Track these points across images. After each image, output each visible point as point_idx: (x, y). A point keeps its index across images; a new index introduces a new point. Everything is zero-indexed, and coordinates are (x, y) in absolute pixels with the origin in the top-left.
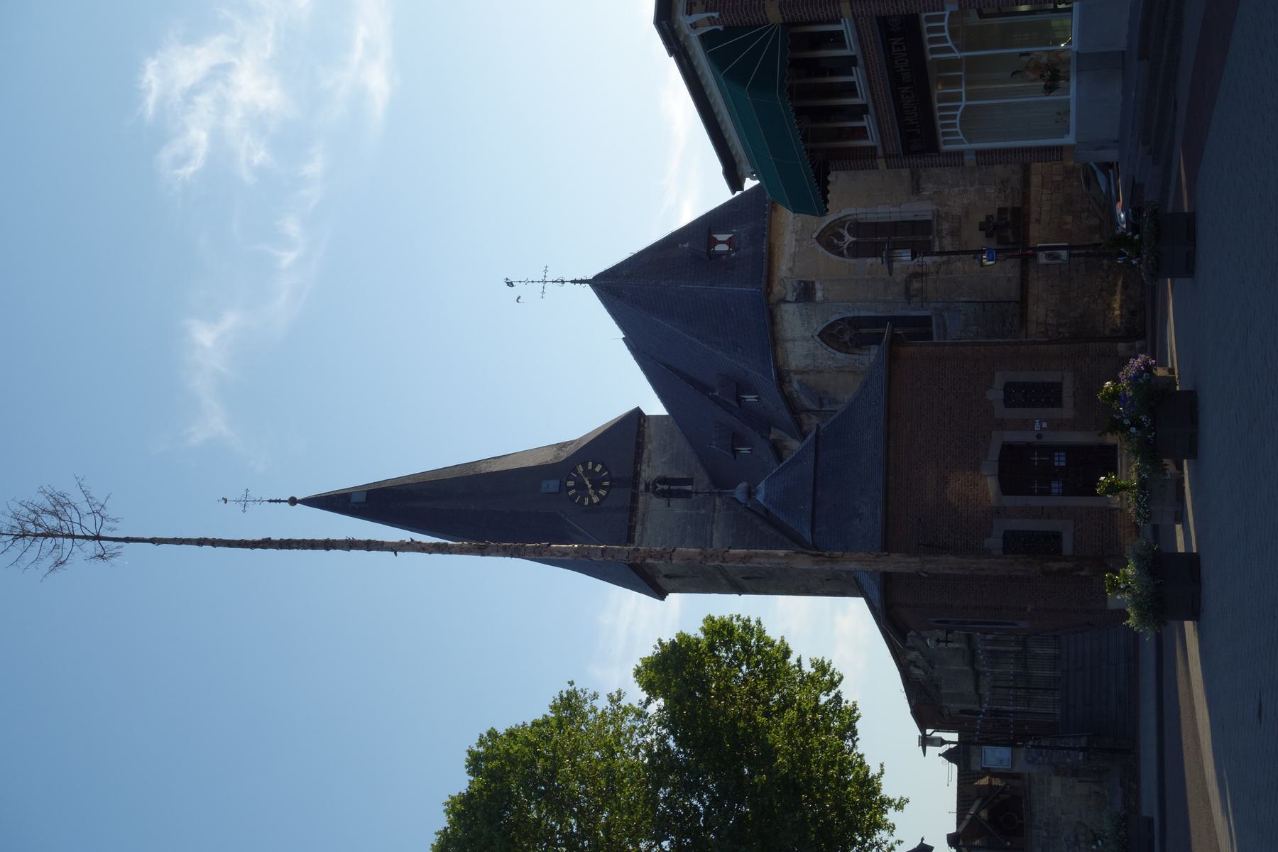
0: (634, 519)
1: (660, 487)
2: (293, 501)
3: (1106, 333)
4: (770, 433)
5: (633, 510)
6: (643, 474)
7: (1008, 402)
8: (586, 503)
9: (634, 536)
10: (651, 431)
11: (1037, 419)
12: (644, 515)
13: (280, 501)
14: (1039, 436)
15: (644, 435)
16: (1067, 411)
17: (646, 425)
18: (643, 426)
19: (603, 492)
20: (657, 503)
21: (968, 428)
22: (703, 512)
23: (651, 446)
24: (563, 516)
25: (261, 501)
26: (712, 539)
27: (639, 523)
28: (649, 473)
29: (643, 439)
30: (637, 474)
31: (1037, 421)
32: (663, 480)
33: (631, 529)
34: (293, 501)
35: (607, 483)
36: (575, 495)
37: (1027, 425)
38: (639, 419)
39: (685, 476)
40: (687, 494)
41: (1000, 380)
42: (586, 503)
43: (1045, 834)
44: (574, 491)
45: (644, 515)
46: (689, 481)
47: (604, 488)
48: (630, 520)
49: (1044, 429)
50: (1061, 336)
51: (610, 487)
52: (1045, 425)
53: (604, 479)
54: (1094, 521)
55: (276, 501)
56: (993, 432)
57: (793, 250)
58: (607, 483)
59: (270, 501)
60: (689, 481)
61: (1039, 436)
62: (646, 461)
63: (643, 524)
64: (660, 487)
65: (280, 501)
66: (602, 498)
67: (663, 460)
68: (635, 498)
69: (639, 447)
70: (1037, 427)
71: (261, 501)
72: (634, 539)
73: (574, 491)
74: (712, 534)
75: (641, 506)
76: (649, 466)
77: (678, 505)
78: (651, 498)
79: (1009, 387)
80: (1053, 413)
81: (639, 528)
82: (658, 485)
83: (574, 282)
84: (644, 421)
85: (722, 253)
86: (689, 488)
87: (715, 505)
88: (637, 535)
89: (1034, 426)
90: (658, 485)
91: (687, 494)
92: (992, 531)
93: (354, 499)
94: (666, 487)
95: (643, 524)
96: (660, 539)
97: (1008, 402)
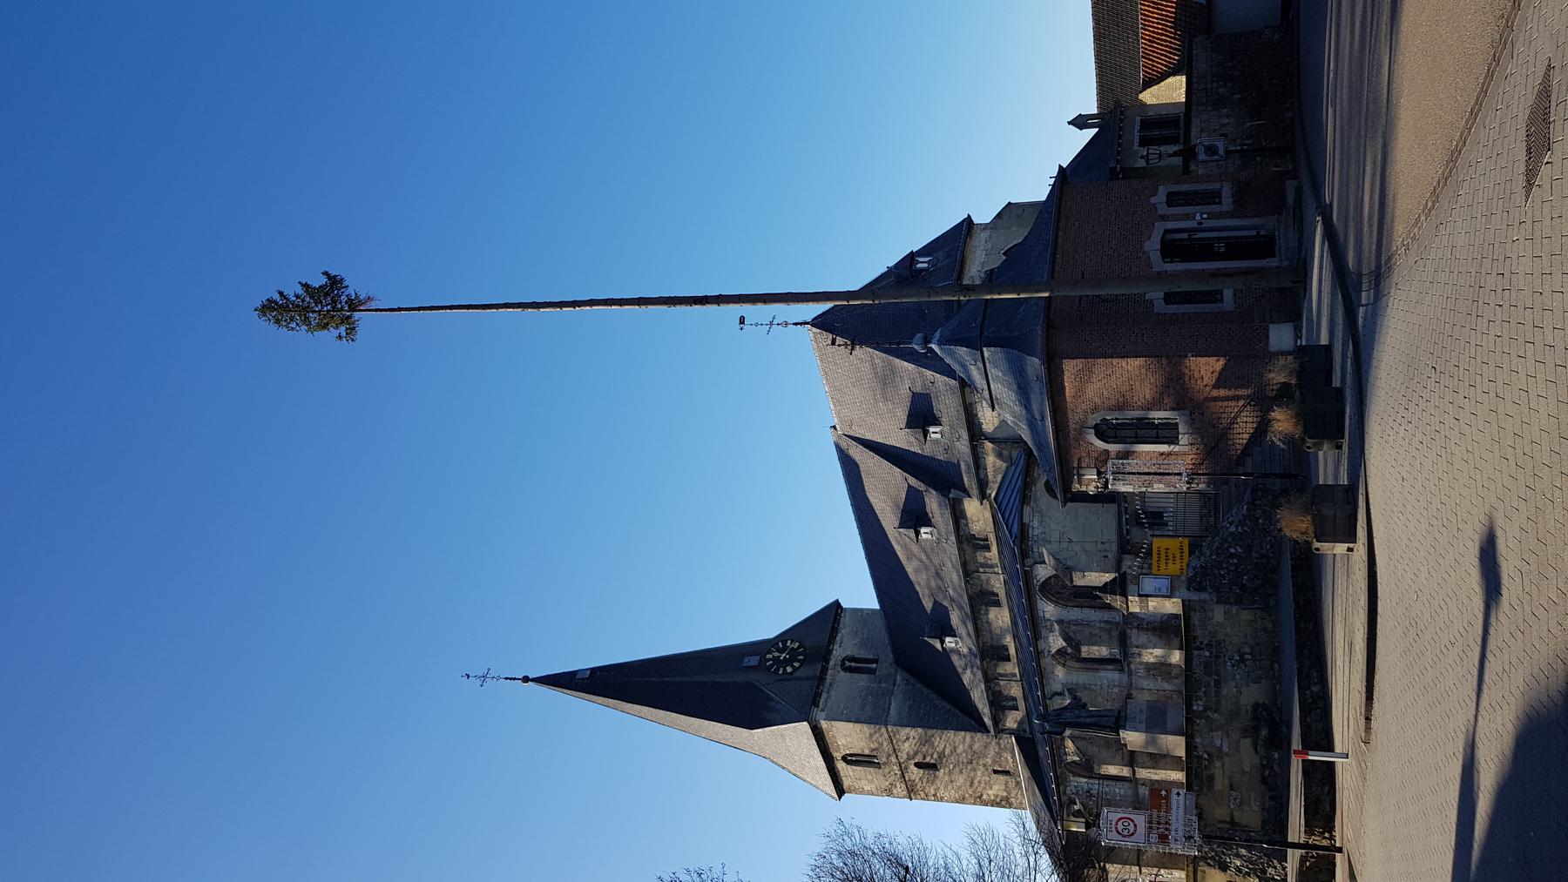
0: (821, 687)
1: (848, 664)
2: (526, 679)
4: (950, 492)
5: (821, 679)
6: (834, 652)
7: (1170, 203)
8: (781, 672)
9: (819, 701)
10: (845, 620)
12: (831, 685)
13: (515, 679)
14: (1200, 223)
15: (839, 622)
16: (1227, 204)
19: (796, 665)
23: (845, 632)
24: (757, 684)
25: (499, 678)
26: (889, 709)
27: (825, 691)
28: (838, 652)
29: (838, 625)
30: (829, 652)
33: (818, 695)
34: (526, 679)
35: (801, 657)
36: (772, 666)
37: (1188, 217)
39: (871, 657)
42: (781, 672)
43: (1208, 654)
44: (771, 662)
45: (831, 685)
46: (875, 661)
47: (799, 661)
48: (818, 687)
51: (804, 660)
55: (511, 679)
57: (982, 260)
58: (801, 657)
59: (506, 678)
63: (828, 693)
64: (848, 664)
65: (515, 679)
66: (795, 669)
67: (854, 642)
68: (824, 670)
69: (834, 631)
70: (1198, 217)
71: (499, 678)
73: (771, 662)
74: (891, 704)
77: (862, 680)
78: (838, 672)
79: (1170, 195)
80: (1214, 208)
81: (824, 695)
82: (846, 662)
83: (794, 324)
84: (841, 612)
85: (922, 270)
86: (874, 665)
87: (895, 681)
88: (822, 700)
90: (846, 662)
91: (872, 672)
93: (579, 676)
94: (853, 664)
95: (828, 693)
97: (1170, 203)
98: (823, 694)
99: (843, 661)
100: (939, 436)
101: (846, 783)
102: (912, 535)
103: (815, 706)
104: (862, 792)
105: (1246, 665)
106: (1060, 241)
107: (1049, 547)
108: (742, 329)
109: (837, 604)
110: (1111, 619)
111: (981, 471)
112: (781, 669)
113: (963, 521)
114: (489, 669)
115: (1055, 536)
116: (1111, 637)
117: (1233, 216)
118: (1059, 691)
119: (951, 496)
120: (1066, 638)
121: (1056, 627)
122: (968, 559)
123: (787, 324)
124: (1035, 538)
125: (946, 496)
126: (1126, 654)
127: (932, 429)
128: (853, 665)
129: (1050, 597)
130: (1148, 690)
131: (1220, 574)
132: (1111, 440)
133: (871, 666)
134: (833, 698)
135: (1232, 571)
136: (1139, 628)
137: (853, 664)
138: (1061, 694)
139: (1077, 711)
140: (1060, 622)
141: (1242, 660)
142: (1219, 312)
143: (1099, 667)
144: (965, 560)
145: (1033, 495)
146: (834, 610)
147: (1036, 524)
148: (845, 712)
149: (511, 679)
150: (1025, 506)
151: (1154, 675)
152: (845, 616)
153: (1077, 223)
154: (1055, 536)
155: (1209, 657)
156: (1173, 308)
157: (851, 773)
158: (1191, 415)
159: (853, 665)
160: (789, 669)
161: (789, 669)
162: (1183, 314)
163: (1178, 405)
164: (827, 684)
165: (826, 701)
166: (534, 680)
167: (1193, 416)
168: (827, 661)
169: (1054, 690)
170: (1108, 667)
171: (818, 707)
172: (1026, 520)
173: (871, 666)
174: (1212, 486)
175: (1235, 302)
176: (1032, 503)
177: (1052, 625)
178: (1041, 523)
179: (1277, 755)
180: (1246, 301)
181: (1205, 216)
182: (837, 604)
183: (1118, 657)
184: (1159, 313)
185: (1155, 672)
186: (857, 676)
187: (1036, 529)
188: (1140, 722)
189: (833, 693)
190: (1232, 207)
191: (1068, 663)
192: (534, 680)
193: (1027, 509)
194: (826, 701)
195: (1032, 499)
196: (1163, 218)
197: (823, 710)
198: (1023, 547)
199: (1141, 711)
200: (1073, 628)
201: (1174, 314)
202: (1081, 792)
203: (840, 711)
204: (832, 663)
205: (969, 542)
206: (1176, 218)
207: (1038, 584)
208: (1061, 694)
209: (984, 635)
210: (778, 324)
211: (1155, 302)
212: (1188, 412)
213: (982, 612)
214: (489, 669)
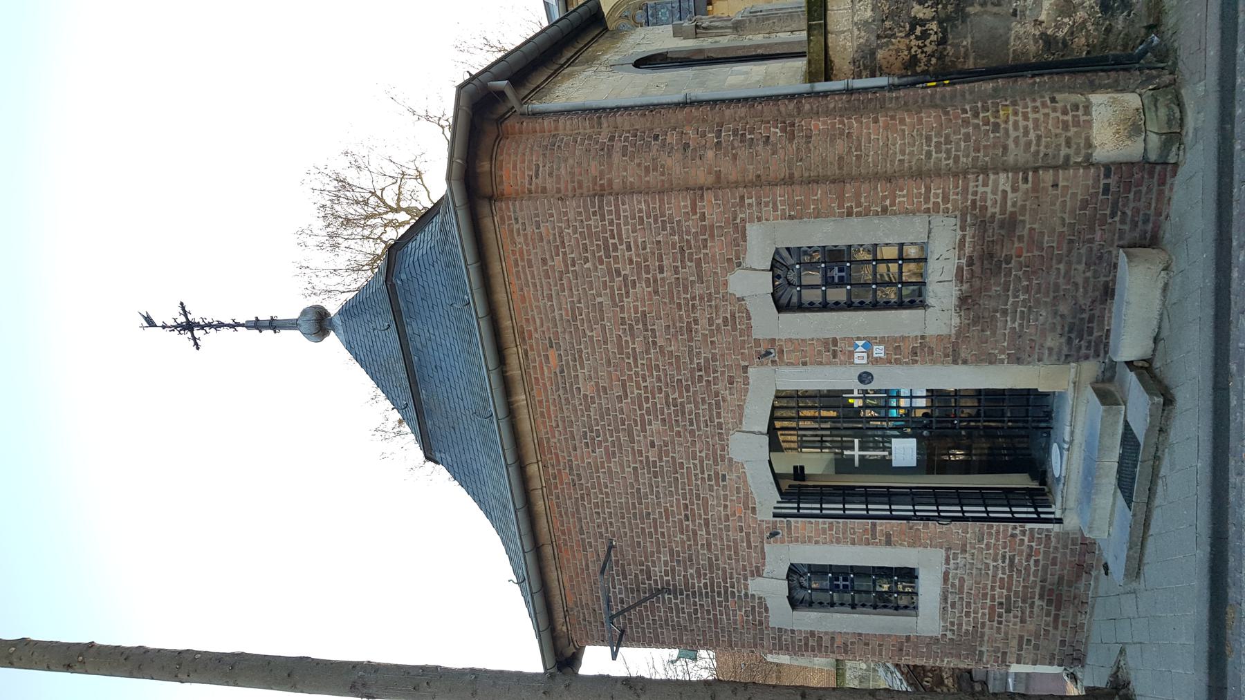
3: (1043, 17)
11: (859, 339)
14: (865, 378)
21: (691, 362)
31: (860, 343)
37: (833, 350)
41: (759, 251)
43: (864, 666)
49: (877, 361)
50: (919, 29)
52: (879, 351)
54: (991, 551)
56: (750, 370)
61: (865, 378)
70: (860, 358)
89: (852, 354)
92: (764, 565)
106: (525, 426)
117: (955, 357)
142: (908, 638)
153: (552, 353)
155: (866, 670)
156: (809, 620)
175: (944, 619)
180: (968, 614)
181: (879, 351)
184: (780, 630)
190: (956, 321)
196: (768, 353)
201: (812, 634)
206: (806, 353)
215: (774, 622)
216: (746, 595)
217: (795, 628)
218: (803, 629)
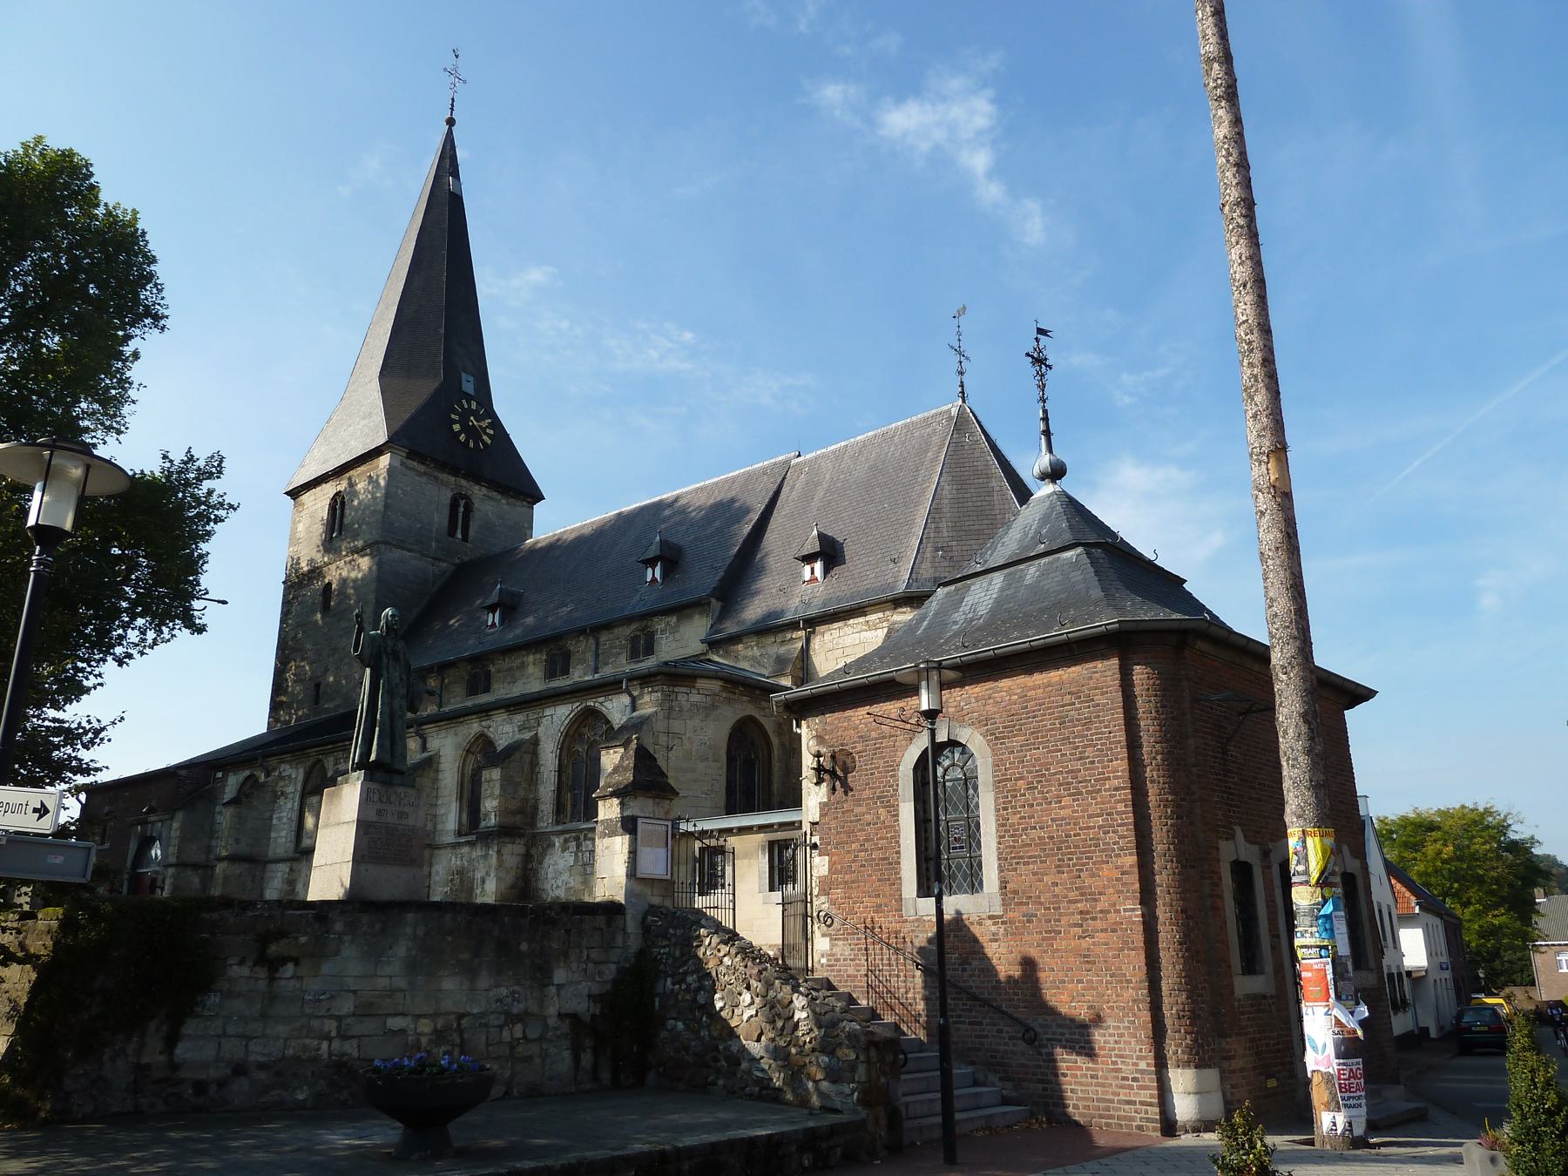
1: (462, 503)
2: (451, 122)
4: (718, 599)
6: (477, 487)
8: (453, 416)
9: (414, 460)
10: (517, 509)
12: (436, 478)
13: (452, 109)
17: (525, 503)
18: (525, 500)
19: (462, 437)
20: (446, 496)
22: (433, 544)
28: (477, 492)
29: (512, 497)
30: (477, 478)
32: (469, 509)
34: (451, 122)
35: (471, 445)
36: (462, 406)
38: (532, 497)
39: (472, 533)
40: (452, 533)
42: (453, 416)
44: (466, 406)
45: (436, 478)
46: (465, 538)
47: (467, 441)
53: (476, 444)
55: (452, 105)
58: (471, 445)
60: (465, 538)
62: (490, 494)
63: (425, 473)
64: (462, 503)
65: (452, 109)
67: (489, 513)
68: (454, 471)
72: (410, 459)
73: (466, 406)
74: (410, 551)
75: (444, 476)
76: (484, 495)
77: (440, 519)
78: (452, 490)
81: (422, 468)
82: (464, 501)
83: (962, 382)
84: (529, 502)
88: (415, 464)
91: (452, 533)
94: (461, 509)
95: (425, 473)
96: (409, 489)
98: (423, 467)
99: (466, 497)
100: (807, 575)
101: (306, 498)
102: (651, 554)
103: (408, 454)
104: (295, 523)
105: (501, 1027)
107: (661, 716)
108: (954, 317)
109: (539, 497)
110: (540, 815)
111: (755, 638)
112: (456, 417)
113: (674, 619)
114: (465, 82)
115: (677, 726)
116: (514, 813)
118: (428, 746)
119: (713, 600)
120: (512, 749)
121: (527, 735)
122: (616, 631)
123: (961, 373)
124: (673, 697)
125: (712, 595)
126: (486, 838)
127: (818, 566)
128: (460, 510)
129: (575, 727)
130: (430, 873)
131: (686, 973)
132: (919, 774)
133: (459, 531)
134: (417, 478)
135: (695, 1000)
136: (527, 857)
137: (461, 509)
138: (424, 748)
139: (403, 691)
140: (535, 742)
141: (512, 1019)
142: (1230, 967)
143: (464, 801)
144: (614, 627)
145: (736, 697)
146: (533, 495)
147: (695, 698)
148: (400, 492)
149: (452, 105)
150: (720, 683)
151: (452, 880)
152: (524, 506)
154: (677, 726)
157: (319, 505)
158: (990, 917)
159: (460, 510)
160: (456, 427)
161: (456, 427)
162: (1220, 897)
163: (1015, 892)
164: (436, 473)
165: (413, 469)
166: (450, 133)
167: (990, 922)
168: (467, 476)
169: (429, 739)
170: (465, 816)
171: (407, 458)
172: (701, 683)
173: (459, 531)
174: (824, 961)
176: (724, 695)
177: (530, 729)
178: (694, 705)
179: (301, 1097)
182: (539, 497)
183: (483, 824)
185: (457, 881)
186: (446, 511)
187: (689, 698)
188: (379, 813)
189: (424, 479)
191: (471, 758)
192: (450, 133)
193: (715, 686)
194: (413, 469)
195: (731, 696)
197: (402, 464)
198: (659, 678)
199: (402, 815)
200: (527, 758)
202: (281, 784)
203: (401, 485)
204: (464, 482)
205: (643, 630)
207: (597, 705)
208: (424, 748)
209: (504, 660)
210: (961, 362)
211: (1231, 842)
212: (998, 911)
213: (538, 656)
214: (465, 82)
215: (1223, 844)
216: (1231, 823)
217: (1221, 863)
218: (1222, 870)
